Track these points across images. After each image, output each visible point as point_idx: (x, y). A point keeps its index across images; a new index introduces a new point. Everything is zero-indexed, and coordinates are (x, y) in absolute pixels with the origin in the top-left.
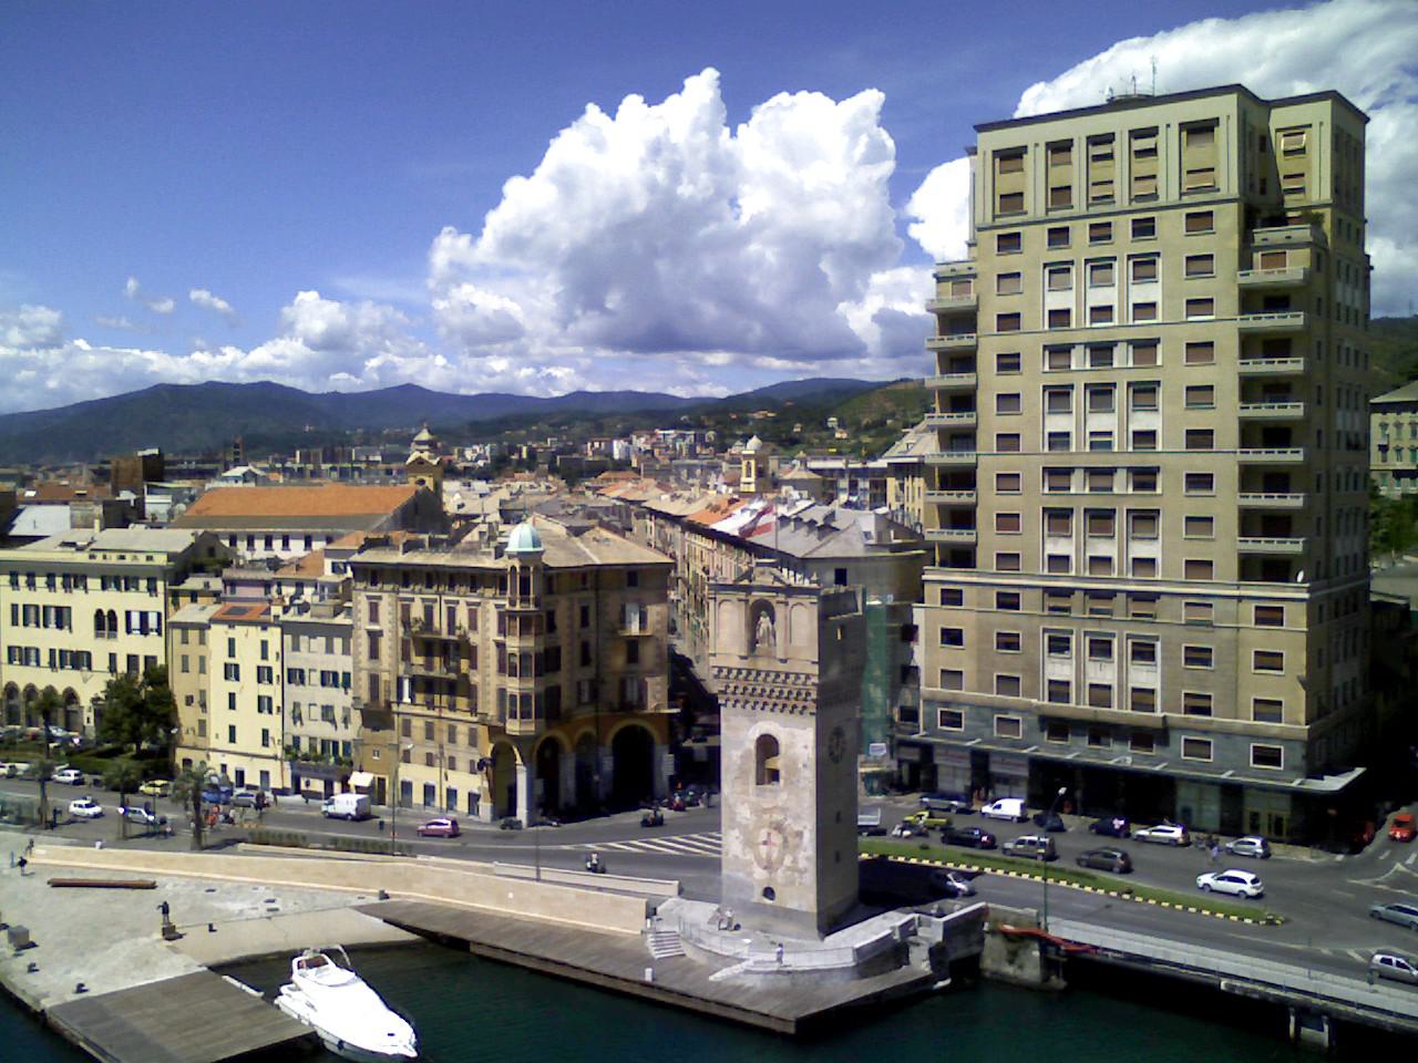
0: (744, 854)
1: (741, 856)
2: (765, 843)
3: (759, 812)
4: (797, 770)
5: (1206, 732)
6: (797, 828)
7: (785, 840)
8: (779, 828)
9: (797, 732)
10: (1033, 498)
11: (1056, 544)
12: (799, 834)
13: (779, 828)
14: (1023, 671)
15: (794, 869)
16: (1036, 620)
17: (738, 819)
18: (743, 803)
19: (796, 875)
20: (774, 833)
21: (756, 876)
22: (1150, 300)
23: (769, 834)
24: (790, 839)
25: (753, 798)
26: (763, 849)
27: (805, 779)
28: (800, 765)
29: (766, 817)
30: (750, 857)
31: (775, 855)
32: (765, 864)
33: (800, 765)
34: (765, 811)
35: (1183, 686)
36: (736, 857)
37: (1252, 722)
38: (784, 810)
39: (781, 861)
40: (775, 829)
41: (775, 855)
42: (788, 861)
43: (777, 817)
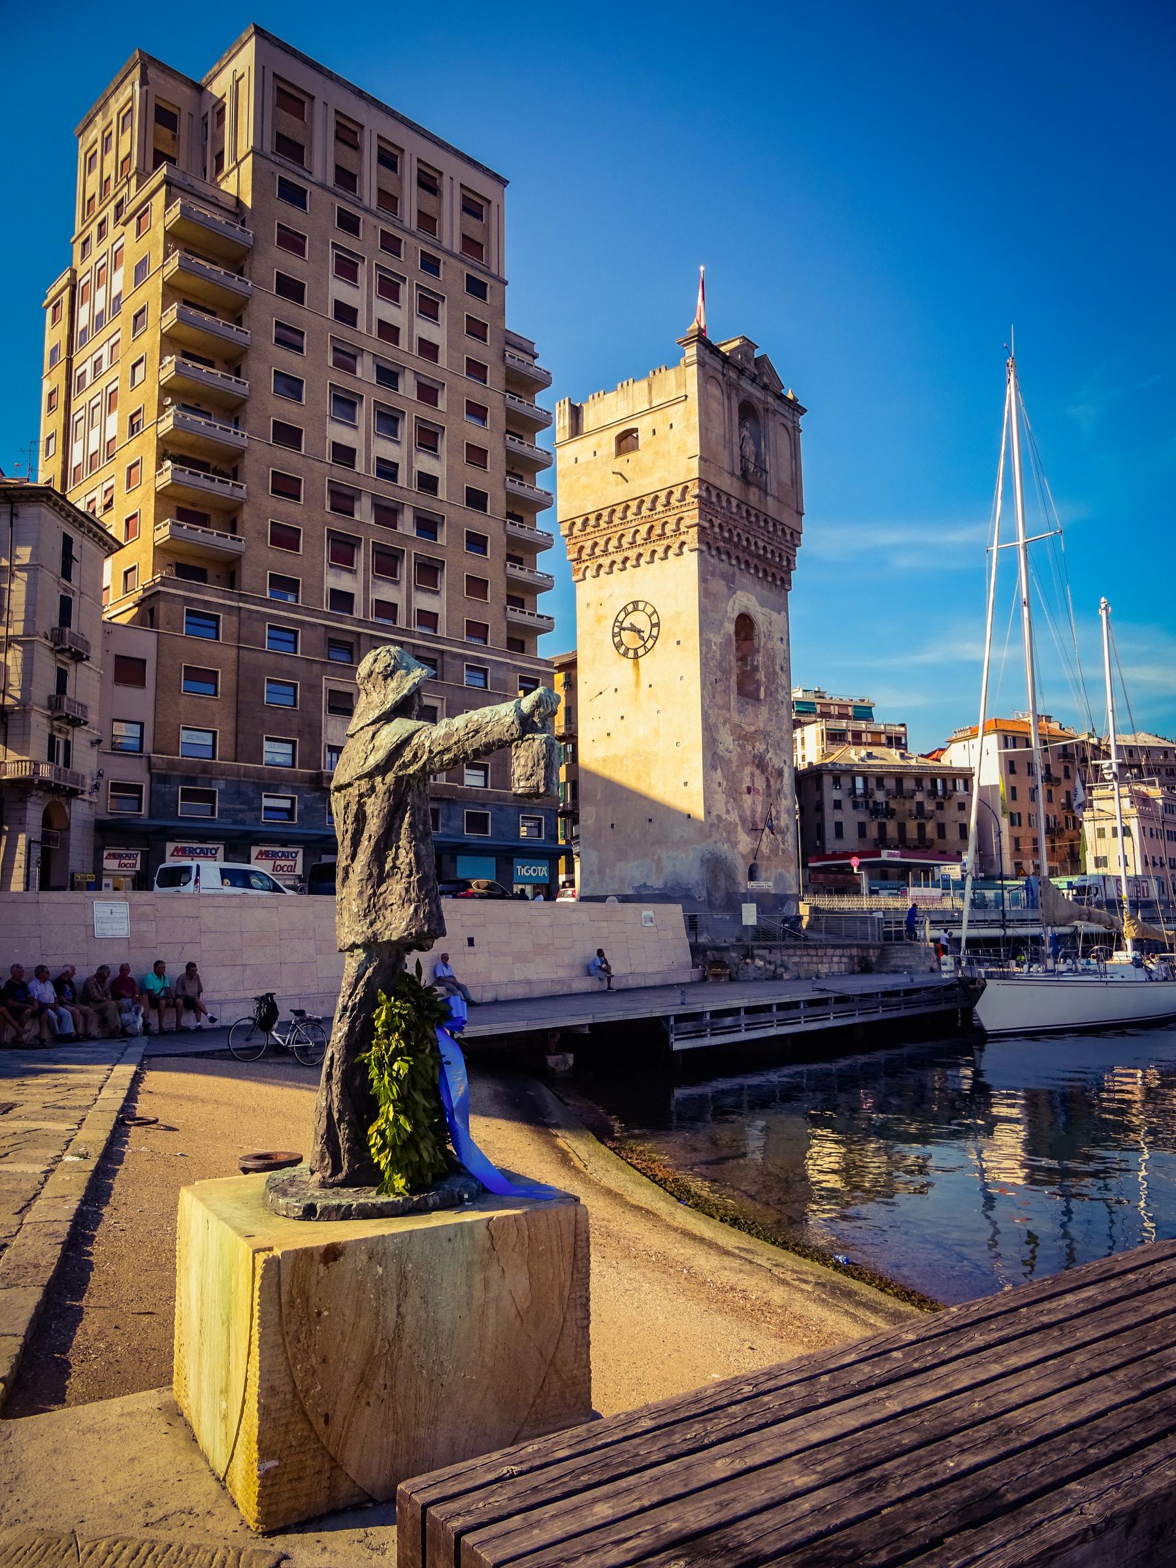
0: (728, 812)
1: (724, 816)
2: (749, 790)
3: (743, 737)
7: (768, 786)
8: (761, 763)
10: (312, 516)
11: (337, 576)
13: (761, 763)
14: (300, 733)
16: (316, 667)
18: (724, 724)
20: (757, 772)
22: (434, 341)
23: (752, 775)
25: (736, 717)
26: (747, 799)
28: (778, 668)
30: (734, 817)
33: (778, 668)
36: (719, 817)
38: (766, 735)
40: (758, 767)
43: (760, 747)
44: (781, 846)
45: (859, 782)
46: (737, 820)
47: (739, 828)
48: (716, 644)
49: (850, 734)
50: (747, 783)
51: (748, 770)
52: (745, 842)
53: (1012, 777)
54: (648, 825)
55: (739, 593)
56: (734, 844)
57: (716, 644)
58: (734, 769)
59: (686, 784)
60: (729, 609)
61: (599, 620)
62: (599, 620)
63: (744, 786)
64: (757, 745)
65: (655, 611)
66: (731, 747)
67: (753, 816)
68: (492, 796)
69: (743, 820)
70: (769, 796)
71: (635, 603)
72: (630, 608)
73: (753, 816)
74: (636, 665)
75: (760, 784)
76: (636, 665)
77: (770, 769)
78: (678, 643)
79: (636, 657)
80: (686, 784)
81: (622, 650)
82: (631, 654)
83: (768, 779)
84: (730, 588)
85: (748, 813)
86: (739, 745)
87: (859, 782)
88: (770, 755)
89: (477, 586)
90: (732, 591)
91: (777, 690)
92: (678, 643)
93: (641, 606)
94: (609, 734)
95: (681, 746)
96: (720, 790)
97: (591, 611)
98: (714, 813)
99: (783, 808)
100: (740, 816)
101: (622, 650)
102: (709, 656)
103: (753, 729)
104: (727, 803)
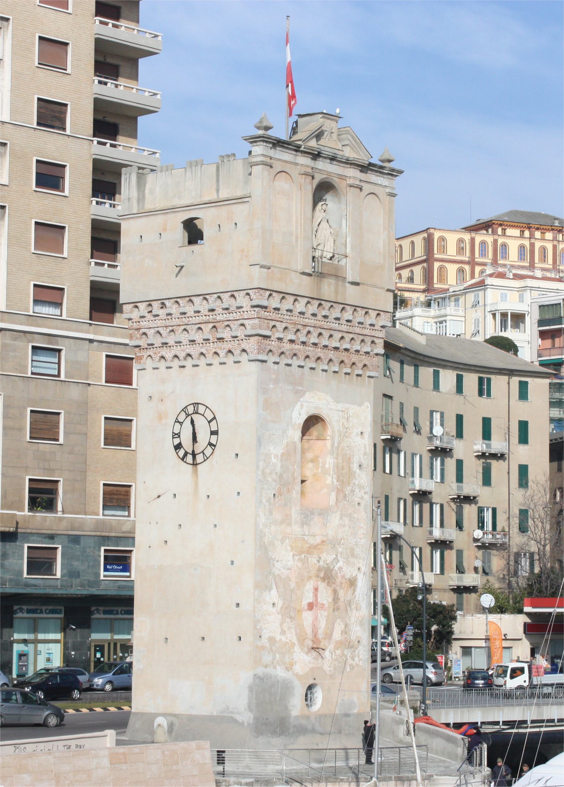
0: (283, 632)
1: (278, 637)
2: (311, 606)
4: (351, 474)
5: (51, 537)
6: (349, 572)
7: (336, 599)
8: (328, 576)
9: (353, 409)
12: (352, 583)
13: (328, 576)
15: (348, 644)
17: (278, 569)
18: (282, 541)
19: (348, 652)
20: (322, 586)
21: (298, 669)
23: (316, 589)
24: (341, 593)
25: (296, 529)
26: (308, 617)
27: (361, 487)
28: (355, 467)
29: (313, 560)
30: (291, 636)
31: (322, 625)
32: (310, 644)
33: (355, 467)
34: (312, 549)
35: (27, 470)
36: (272, 640)
37: (101, 517)
38: (334, 543)
39: (329, 636)
40: (323, 579)
41: (322, 625)
42: (337, 635)
43: (328, 557)
44: (350, 661)
46: (295, 640)
47: (297, 648)
48: (276, 456)
50: (309, 598)
51: (309, 586)
52: (303, 661)
55: (307, 395)
57: (276, 456)
58: (293, 585)
59: (238, 605)
60: (295, 414)
62: (160, 417)
63: (305, 603)
64: (324, 556)
66: (290, 563)
67: (315, 635)
68: (64, 524)
69: (301, 639)
70: (336, 609)
71: (196, 404)
73: (315, 635)
74: (196, 472)
75: (325, 596)
77: (338, 581)
79: (195, 464)
80: (238, 605)
81: (181, 453)
83: (335, 592)
84: (297, 392)
85: (309, 631)
86: (300, 560)
88: (340, 564)
89: (49, 233)
90: (299, 394)
91: (353, 491)
96: (274, 610)
98: (266, 635)
99: (353, 619)
101: (181, 453)
102: (268, 471)
103: (318, 540)
104: (281, 624)
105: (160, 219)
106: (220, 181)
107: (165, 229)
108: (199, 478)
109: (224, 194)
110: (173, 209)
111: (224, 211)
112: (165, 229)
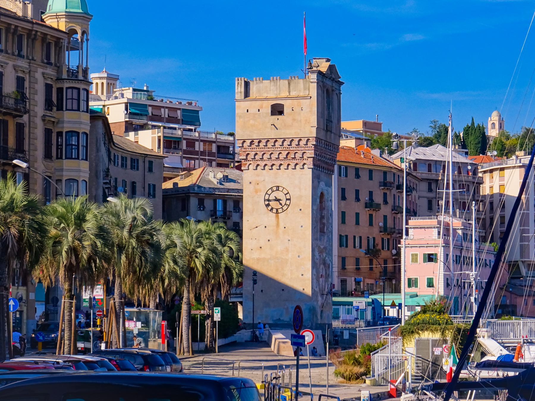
45: (220, 203)
49: (184, 142)
53: (343, 202)
54: (282, 292)
56: (317, 301)
59: (302, 275)
61: (256, 191)
62: (256, 191)
65: (288, 193)
72: (275, 189)
74: (277, 217)
76: (277, 217)
78: (300, 210)
80: (302, 275)
82: (274, 211)
87: (220, 203)
88: (327, 258)
92: (300, 210)
93: (281, 189)
94: (261, 247)
95: (301, 257)
97: (251, 186)
100: (319, 289)
101: (270, 208)
105: (259, 103)
106: (291, 88)
107: (262, 107)
108: (280, 219)
109: (293, 94)
110: (266, 99)
111: (295, 102)
112: (262, 107)
